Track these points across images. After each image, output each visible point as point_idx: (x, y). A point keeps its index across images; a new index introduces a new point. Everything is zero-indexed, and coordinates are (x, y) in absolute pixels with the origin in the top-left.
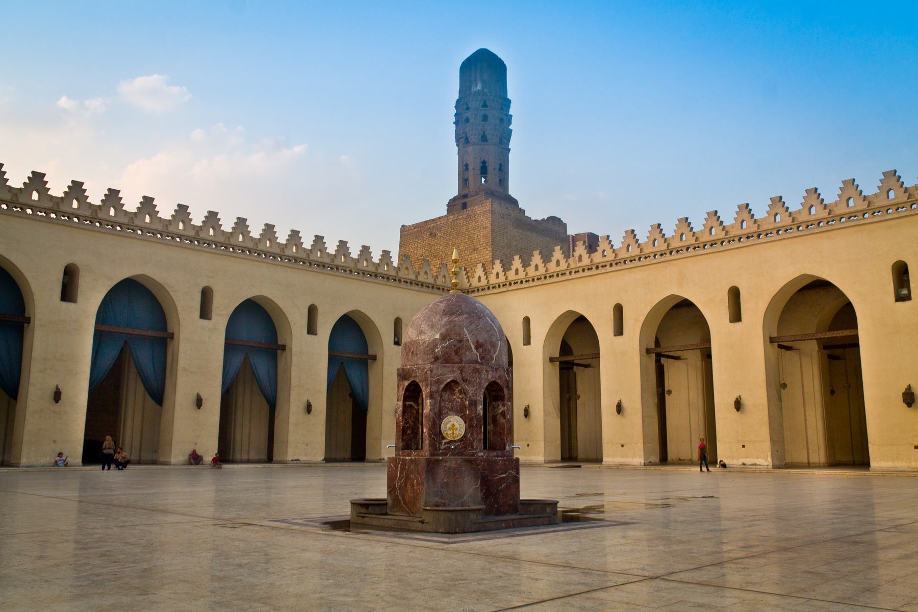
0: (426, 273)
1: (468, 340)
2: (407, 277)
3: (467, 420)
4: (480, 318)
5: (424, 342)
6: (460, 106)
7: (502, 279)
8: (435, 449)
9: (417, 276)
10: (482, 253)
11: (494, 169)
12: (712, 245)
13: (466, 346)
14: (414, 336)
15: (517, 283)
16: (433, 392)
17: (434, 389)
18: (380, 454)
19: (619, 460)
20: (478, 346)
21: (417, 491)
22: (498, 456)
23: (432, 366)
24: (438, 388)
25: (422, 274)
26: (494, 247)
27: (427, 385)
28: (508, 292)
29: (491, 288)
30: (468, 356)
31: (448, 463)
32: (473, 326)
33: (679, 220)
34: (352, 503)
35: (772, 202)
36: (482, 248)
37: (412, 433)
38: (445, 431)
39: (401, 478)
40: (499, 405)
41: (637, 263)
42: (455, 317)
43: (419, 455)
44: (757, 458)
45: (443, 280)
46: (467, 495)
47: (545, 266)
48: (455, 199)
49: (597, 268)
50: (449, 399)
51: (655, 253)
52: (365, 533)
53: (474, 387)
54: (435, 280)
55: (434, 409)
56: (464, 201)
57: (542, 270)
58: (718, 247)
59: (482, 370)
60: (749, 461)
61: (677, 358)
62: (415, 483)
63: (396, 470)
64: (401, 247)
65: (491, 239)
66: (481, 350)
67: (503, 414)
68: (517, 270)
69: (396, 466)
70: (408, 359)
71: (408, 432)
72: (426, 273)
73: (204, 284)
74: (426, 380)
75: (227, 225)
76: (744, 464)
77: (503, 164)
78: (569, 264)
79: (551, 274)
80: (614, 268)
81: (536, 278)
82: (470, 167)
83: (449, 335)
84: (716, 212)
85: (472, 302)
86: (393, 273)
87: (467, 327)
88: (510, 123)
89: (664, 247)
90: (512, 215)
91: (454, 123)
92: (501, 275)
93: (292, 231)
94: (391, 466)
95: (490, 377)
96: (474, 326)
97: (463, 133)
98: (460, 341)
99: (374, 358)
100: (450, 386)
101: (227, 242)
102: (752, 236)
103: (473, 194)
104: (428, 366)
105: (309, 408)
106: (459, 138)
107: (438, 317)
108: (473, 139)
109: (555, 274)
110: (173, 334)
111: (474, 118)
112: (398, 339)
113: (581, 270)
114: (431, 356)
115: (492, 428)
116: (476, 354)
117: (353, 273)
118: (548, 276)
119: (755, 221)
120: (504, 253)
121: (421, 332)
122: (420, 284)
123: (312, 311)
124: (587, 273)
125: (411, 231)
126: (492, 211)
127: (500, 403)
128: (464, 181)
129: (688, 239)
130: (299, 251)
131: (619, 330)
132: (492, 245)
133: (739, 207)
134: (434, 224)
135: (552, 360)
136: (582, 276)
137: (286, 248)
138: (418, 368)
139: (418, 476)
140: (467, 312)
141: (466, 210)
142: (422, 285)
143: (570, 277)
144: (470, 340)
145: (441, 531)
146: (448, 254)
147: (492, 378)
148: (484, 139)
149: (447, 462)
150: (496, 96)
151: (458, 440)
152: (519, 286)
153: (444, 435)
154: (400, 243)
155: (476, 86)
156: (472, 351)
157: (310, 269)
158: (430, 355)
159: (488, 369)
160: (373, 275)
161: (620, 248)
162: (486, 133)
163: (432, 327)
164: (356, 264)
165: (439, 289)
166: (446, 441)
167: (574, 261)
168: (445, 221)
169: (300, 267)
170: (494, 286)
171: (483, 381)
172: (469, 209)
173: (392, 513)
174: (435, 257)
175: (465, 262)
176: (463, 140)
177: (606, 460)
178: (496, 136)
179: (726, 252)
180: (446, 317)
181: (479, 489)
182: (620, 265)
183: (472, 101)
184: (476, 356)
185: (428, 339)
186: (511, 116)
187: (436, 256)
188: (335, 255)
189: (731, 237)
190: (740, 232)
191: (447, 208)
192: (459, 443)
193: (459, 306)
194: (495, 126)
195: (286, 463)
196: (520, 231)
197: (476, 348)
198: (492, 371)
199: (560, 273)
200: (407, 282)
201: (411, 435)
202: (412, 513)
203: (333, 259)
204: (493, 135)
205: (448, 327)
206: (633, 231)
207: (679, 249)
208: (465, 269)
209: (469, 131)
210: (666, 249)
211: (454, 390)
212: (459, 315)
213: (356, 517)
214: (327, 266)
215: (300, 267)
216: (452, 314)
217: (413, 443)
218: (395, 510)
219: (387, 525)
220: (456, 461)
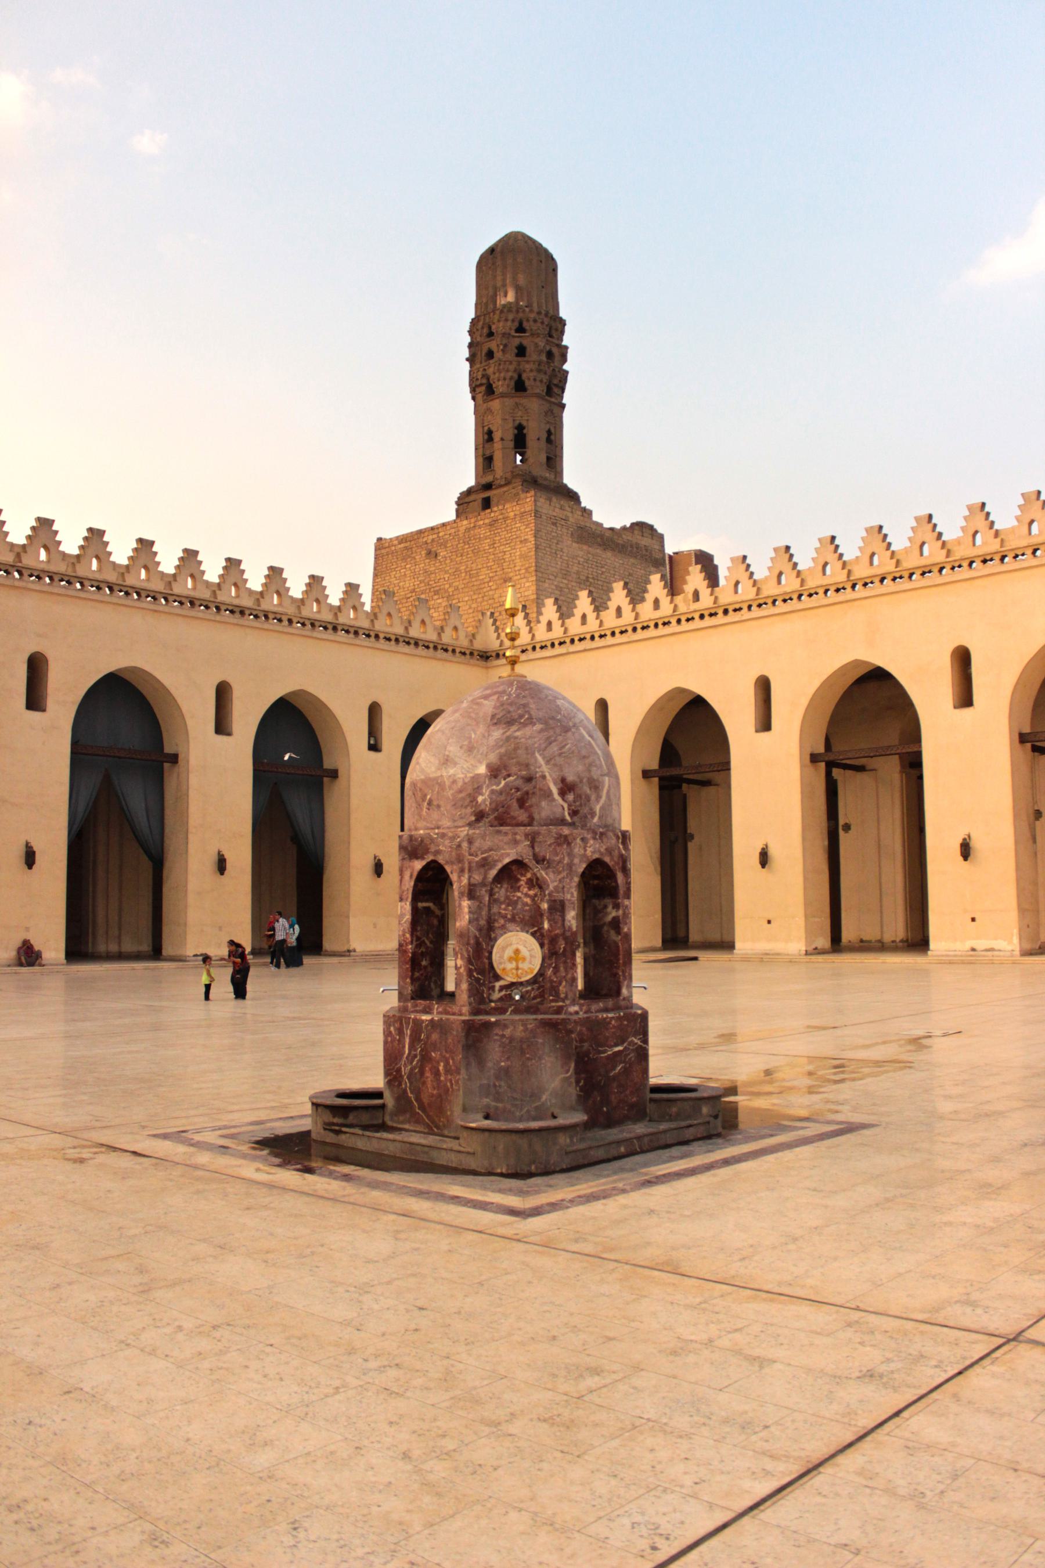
0: (423, 622)
1: (544, 777)
2: (390, 630)
3: (546, 942)
4: (566, 730)
5: (454, 782)
6: (477, 330)
7: (557, 632)
8: (482, 1000)
9: (406, 629)
10: (519, 586)
11: (538, 439)
12: (923, 574)
13: (540, 789)
14: (433, 769)
15: (584, 638)
16: (474, 885)
17: (477, 878)
18: (348, 941)
19: (763, 946)
20: (566, 788)
21: (445, 1085)
22: (606, 1010)
23: (471, 832)
24: (485, 878)
25: (416, 624)
26: (540, 575)
27: (462, 871)
28: (568, 656)
29: (538, 646)
30: (545, 810)
31: (509, 1030)
32: (554, 748)
33: (867, 530)
34: (313, 1104)
35: (1025, 500)
36: (519, 577)
37: (432, 964)
38: (501, 963)
39: (411, 1058)
40: (605, 907)
41: (794, 604)
42: (518, 730)
43: (447, 1013)
44: (996, 939)
46: (549, 1092)
47: (633, 610)
48: (469, 492)
49: (726, 612)
50: (507, 897)
51: (827, 587)
52: (347, 1177)
53: (560, 873)
54: (439, 634)
55: (477, 919)
56: (486, 494)
57: (628, 617)
58: (933, 578)
59: (575, 839)
60: (981, 944)
61: (860, 769)
62: (441, 1068)
63: (401, 1041)
64: (375, 575)
65: (533, 560)
66: (570, 797)
67: (616, 924)
68: (584, 617)
69: (400, 1031)
70: (420, 816)
71: (424, 963)
72: (423, 622)
73: (33, 648)
74: (460, 860)
75: (71, 543)
76: (973, 950)
77: (553, 430)
78: (676, 606)
79: (645, 624)
80: (756, 612)
81: (617, 631)
82: (497, 436)
83: (505, 767)
84: (930, 517)
85: (550, 698)
86: (365, 624)
87: (542, 751)
88: (564, 359)
89: (842, 577)
90: (571, 519)
91: (467, 360)
92: (557, 624)
93: (186, 551)
94: (390, 1032)
95: (589, 850)
96: (555, 749)
97: (483, 376)
98: (529, 779)
99: (334, 774)
100: (510, 873)
101: (70, 572)
102: (991, 560)
103: (503, 483)
104: (464, 832)
105: (221, 865)
106: (477, 386)
107: (481, 729)
108: (500, 387)
109: (652, 624)
111: (503, 351)
112: (376, 740)
113: (697, 616)
114: (469, 810)
115: (593, 952)
116: (560, 805)
117: (294, 625)
118: (639, 626)
119: (997, 534)
120: (556, 586)
121: (447, 761)
122: (412, 642)
123: (223, 693)
124: (708, 621)
125: (393, 548)
126: (536, 512)
127: (608, 901)
128: (485, 461)
129: (883, 564)
130: (199, 586)
131: (765, 724)
132: (536, 571)
133: (970, 508)
134: (435, 536)
135: (646, 774)
136: (699, 627)
137: (175, 580)
138: (443, 836)
139: (448, 1055)
140: (540, 719)
141: (489, 511)
142: (416, 644)
143: (679, 629)
144: (548, 777)
145: (499, 1171)
146: (460, 587)
147: (593, 853)
148: (520, 386)
149: (505, 1026)
150: (539, 313)
151: (527, 981)
152: (587, 644)
153: (499, 972)
154: (375, 569)
155: (506, 296)
156: (554, 800)
157: (218, 618)
158: (466, 807)
159: (586, 835)
160: (330, 627)
161: (766, 578)
162: (524, 376)
163: (470, 749)
164: (299, 607)
165: (446, 650)
166: (502, 983)
167: (685, 600)
168: (453, 530)
169: (200, 615)
170: (543, 644)
171: (576, 861)
173: (395, 1125)
174: (436, 593)
175: (490, 602)
176: (483, 388)
177: (742, 945)
178: (541, 381)
179: (948, 587)
180: (498, 729)
181: (573, 1080)
182: (766, 608)
183: (499, 321)
184: (560, 810)
185: (462, 776)
186: (566, 348)
187: (437, 591)
188: (261, 593)
189: (955, 561)
190: (971, 553)
191: (455, 507)
192: (529, 988)
193: (525, 706)
194: (539, 365)
195: (185, 961)
196: (585, 547)
197: (562, 793)
198: (594, 838)
199: (660, 622)
200: (389, 639)
201: (429, 969)
202: (438, 1127)
203: (258, 600)
204: (535, 380)
205: (503, 750)
206: (788, 548)
207: (868, 581)
208: (492, 614)
209: (494, 373)
210: (845, 579)
211: (519, 880)
212: (525, 725)
213: (322, 1131)
214: (247, 612)
215: (200, 615)
216: (510, 723)
217: (432, 985)
218: (401, 1118)
219: (386, 1152)
220: (525, 1025)
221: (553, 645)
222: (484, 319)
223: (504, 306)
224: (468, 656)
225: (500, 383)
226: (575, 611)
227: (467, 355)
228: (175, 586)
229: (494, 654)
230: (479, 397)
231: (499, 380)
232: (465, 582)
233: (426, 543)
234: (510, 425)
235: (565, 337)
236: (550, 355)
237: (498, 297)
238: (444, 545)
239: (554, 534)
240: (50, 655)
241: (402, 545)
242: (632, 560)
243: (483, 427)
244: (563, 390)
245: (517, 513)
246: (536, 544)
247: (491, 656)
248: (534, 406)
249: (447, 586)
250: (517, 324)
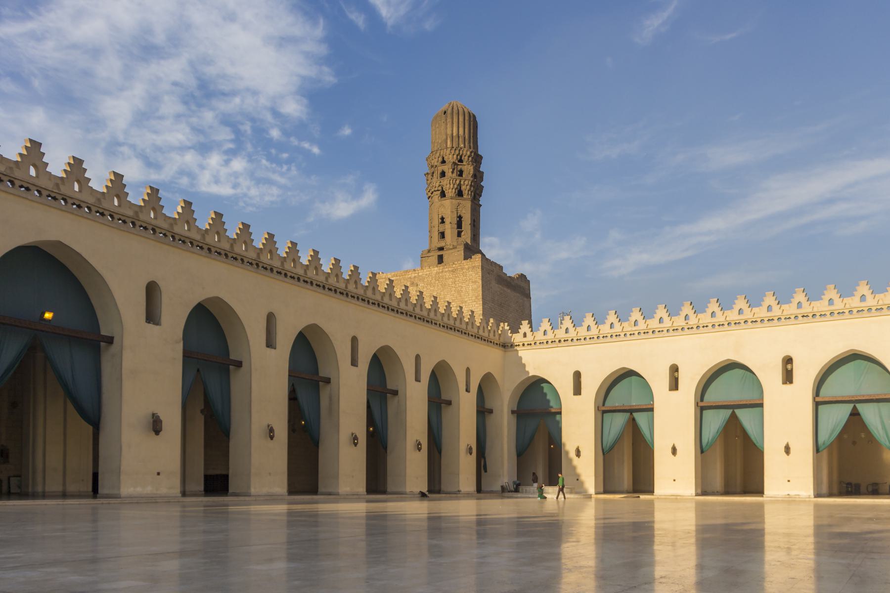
6: (435, 158)
36: (471, 301)
48: (429, 251)
73: (353, 334)
77: (476, 219)
82: (447, 221)
97: (439, 186)
99: (449, 403)
103: (451, 247)
106: (435, 191)
110: (330, 379)
111: (453, 172)
126: (482, 266)
132: (483, 298)
148: (460, 194)
160: (453, 328)
162: (463, 188)
167: (629, 325)
168: (428, 273)
172: (456, 263)
176: (439, 192)
183: (449, 154)
186: (483, 173)
196: (500, 286)
209: (447, 185)
221: (547, 342)
222: (440, 153)
228: (401, 304)
229: (509, 345)
239: (488, 279)
240: (359, 338)
242: (518, 295)
244: (481, 196)
245: (470, 266)
247: (508, 346)
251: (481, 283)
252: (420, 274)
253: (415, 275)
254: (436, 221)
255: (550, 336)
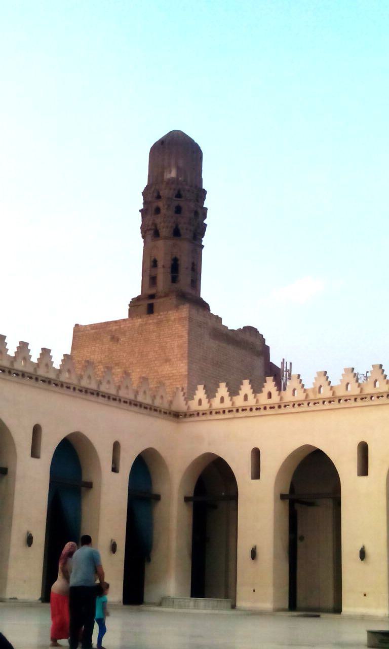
11: (187, 268)
29: (214, 412)
36: (176, 359)
45: (161, 401)
48: (138, 298)
65: (186, 350)
82: (160, 264)
88: (205, 217)
108: (164, 232)
126: (190, 318)
132: (188, 356)
134: (117, 327)
148: (176, 233)
150: (191, 186)
155: (170, 173)
162: (180, 226)
165: (156, 410)
168: (130, 325)
175: (155, 374)
176: (152, 232)
178: (190, 231)
186: (206, 209)
191: (129, 308)
196: (217, 342)
204: (187, 229)
209: (161, 223)
223: (169, 180)
224: (168, 414)
225: (164, 230)
226: (240, 392)
227: (142, 207)
229: (183, 414)
230: (149, 237)
231: (163, 228)
232: (137, 359)
233: (111, 331)
234: (169, 258)
235: (205, 202)
236: (196, 213)
237: (165, 174)
238: (124, 333)
241: (94, 331)
243: (151, 257)
244: (203, 235)
246: (188, 339)
248: (185, 246)
249: (124, 361)
250: (176, 192)
251: (187, 338)
252: (122, 326)
253: (117, 327)
254: (148, 264)
255: (251, 401)
